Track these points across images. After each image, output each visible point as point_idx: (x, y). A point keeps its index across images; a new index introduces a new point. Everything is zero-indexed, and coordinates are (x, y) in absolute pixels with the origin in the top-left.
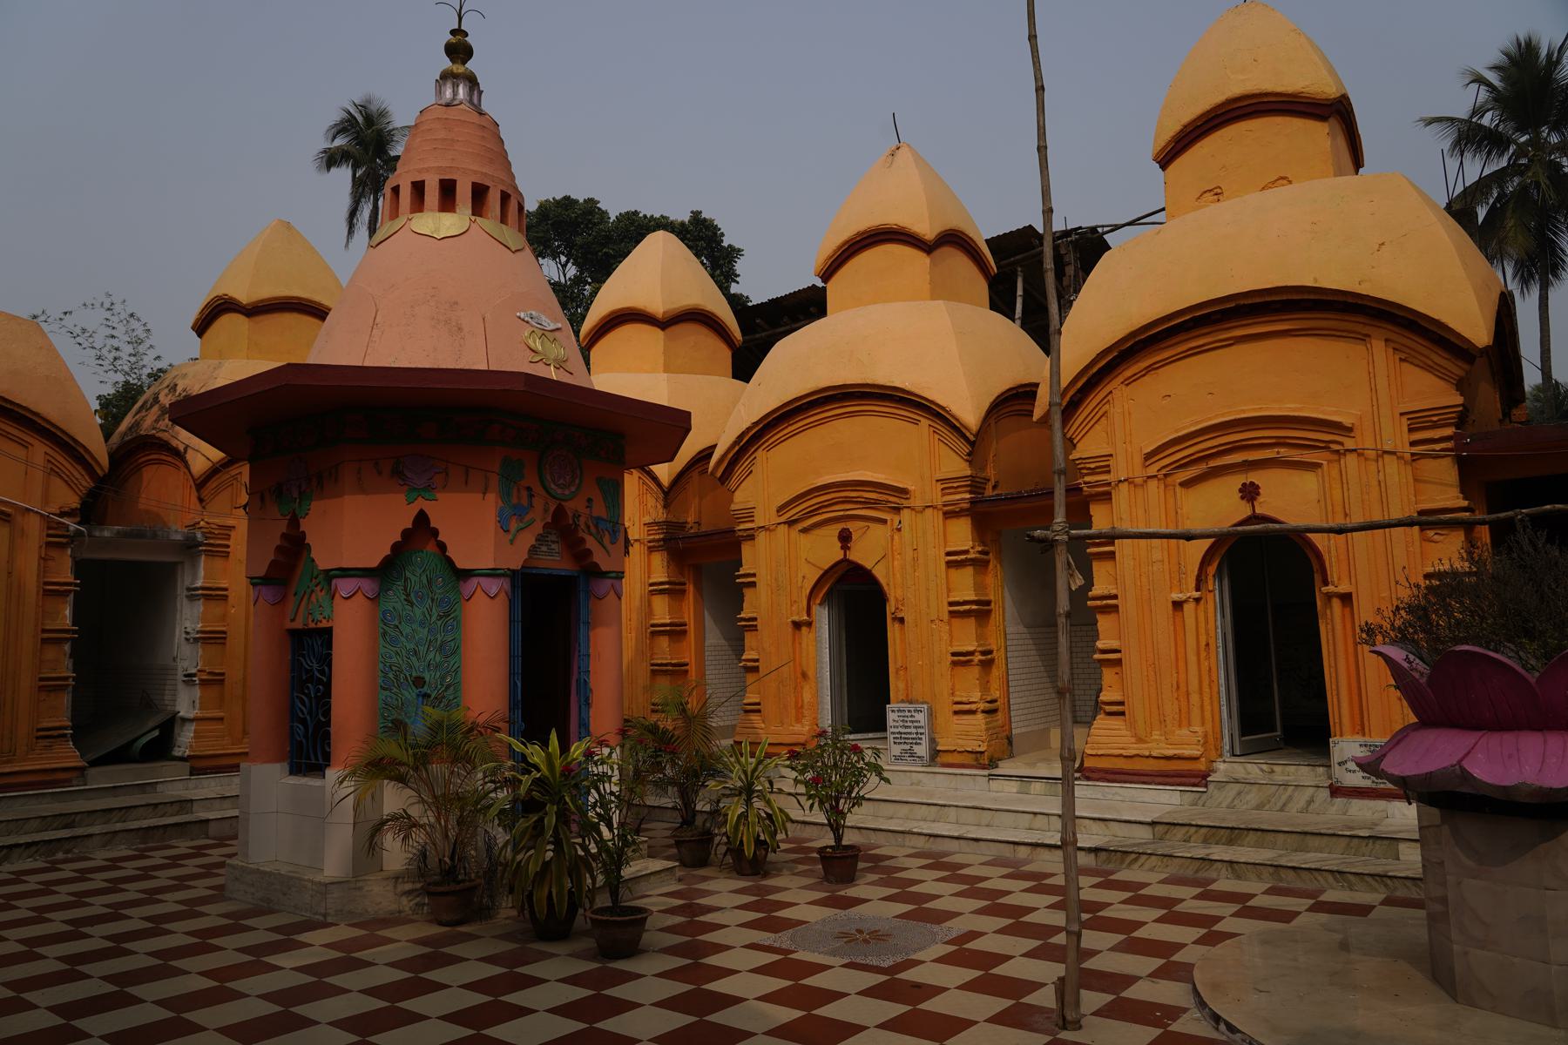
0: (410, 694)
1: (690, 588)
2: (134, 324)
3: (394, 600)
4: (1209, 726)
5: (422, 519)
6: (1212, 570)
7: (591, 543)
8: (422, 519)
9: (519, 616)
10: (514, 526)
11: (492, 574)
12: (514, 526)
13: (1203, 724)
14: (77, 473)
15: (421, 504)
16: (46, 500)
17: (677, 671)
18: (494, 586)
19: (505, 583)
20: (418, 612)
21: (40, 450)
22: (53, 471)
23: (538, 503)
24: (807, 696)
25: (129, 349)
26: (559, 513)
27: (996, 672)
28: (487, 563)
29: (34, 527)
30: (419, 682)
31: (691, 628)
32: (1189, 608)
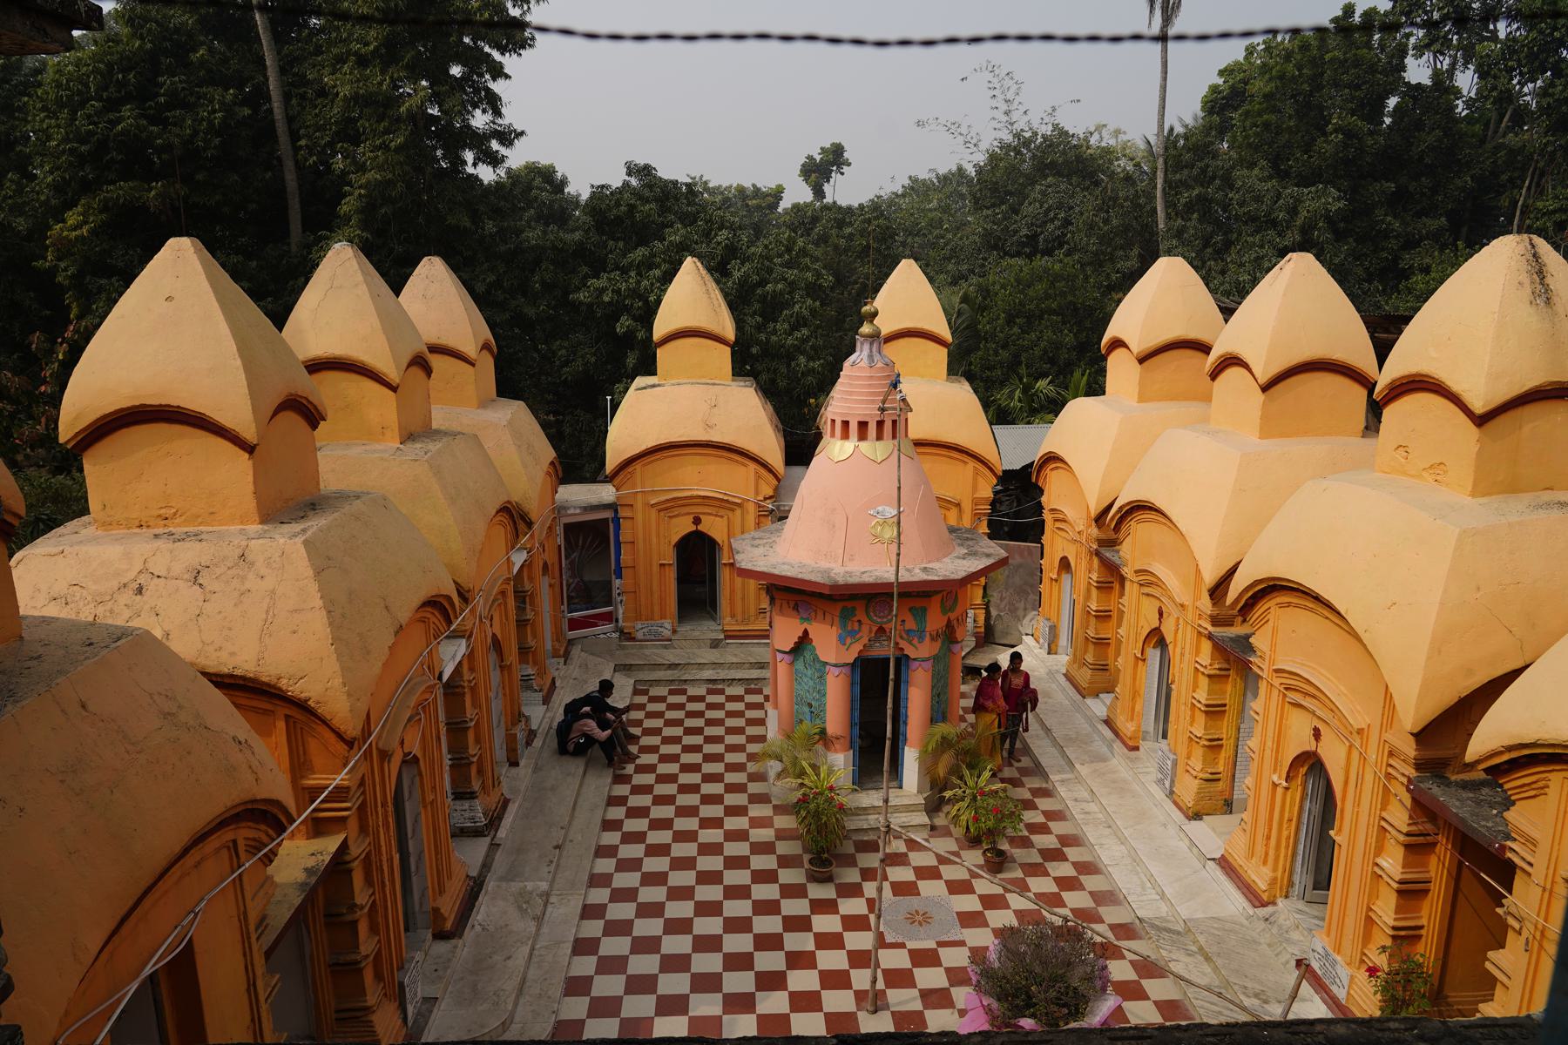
0: (806, 709)
1: (1117, 586)
2: (1008, 82)
3: (799, 665)
4: (1279, 874)
5: (806, 632)
6: (1303, 770)
7: (902, 644)
8: (806, 632)
9: (858, 679)
10: (849, 641)
11: (835, 666)
12: (849, 641)
13: (1275, 870)
14: (770, 477)
15: (806, 625)
16: (757, 493)
17: (1101, 643)
18: (836, 671)
19: (846, 670)
20: (809, 672)
21: (752, 466)
22: (758, 477)
23: (865, 629)
24: (1138, 708)
25: (1004, 107)
26: (881, 630)
27: (1224, 755)
28: (833, 661)
29: (751, 508)
30: (810, 706)
31: (1115, 614)
32: (1280, 790)
